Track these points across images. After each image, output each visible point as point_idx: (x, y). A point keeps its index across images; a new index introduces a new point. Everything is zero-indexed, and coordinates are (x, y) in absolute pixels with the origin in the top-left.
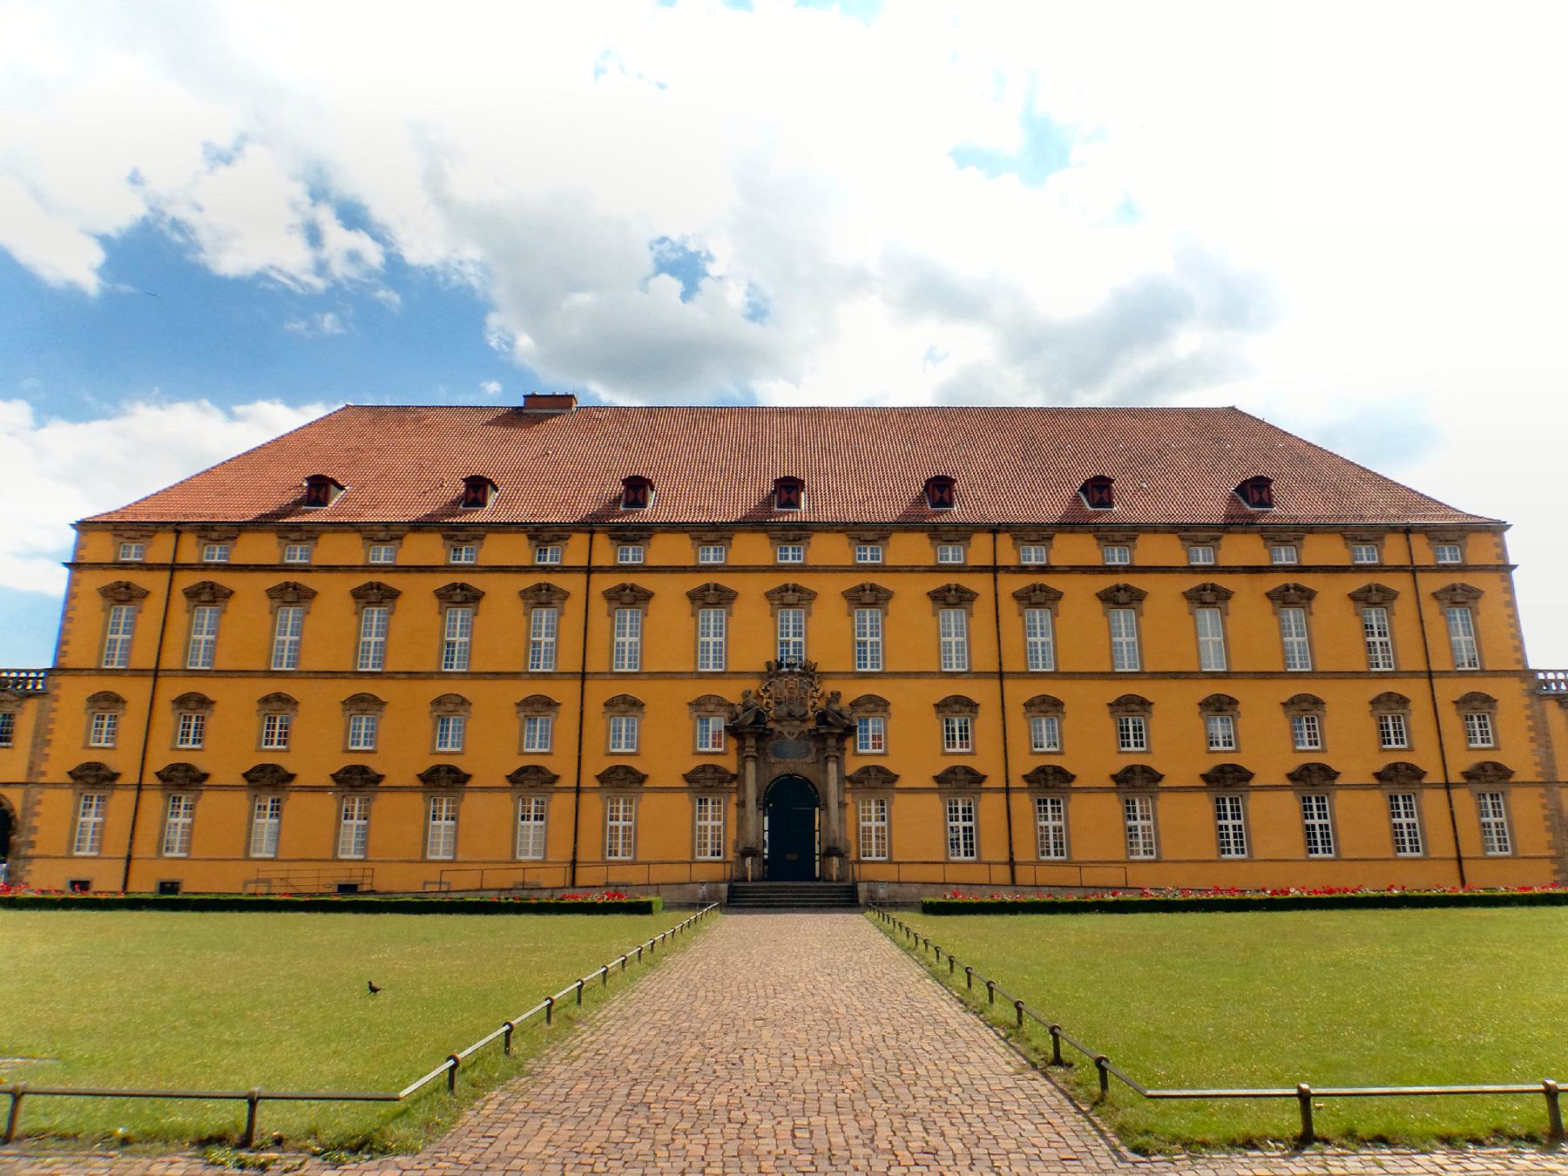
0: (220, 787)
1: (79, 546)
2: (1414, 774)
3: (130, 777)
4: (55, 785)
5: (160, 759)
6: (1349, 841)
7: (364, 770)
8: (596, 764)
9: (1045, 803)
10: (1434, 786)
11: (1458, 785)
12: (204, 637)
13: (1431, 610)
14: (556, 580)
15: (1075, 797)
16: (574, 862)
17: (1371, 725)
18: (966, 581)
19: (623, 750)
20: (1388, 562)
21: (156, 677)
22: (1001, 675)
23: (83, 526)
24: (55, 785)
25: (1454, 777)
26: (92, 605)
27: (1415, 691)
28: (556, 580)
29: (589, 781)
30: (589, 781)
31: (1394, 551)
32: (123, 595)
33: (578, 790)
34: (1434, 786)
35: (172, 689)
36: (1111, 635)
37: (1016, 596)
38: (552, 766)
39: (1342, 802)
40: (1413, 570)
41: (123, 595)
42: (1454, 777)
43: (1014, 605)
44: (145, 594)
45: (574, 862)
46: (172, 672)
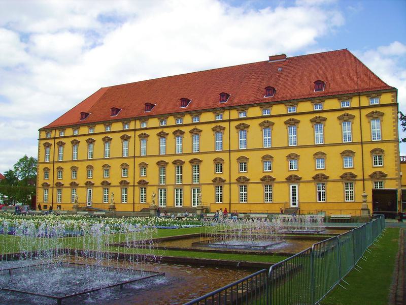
0: (65, 187)
1: (40, 136)
3: (51, 186)
4: (82, 187)
6: (329, 198)
7: (125, 181)
8: (137, 180)
9: (348, 184)
10: (360, 180)
11: (367, 180)
12: (75, 152)
15: (387, 181)
16: (134, 204)
22: (230, 151)
23: (40, 130)
24: (82, 187)
25: (366, 177)
26: (42, 147)
27: (356, 149)
29: (136, 184)
30: (136, 184)
31: (355, 102)
32: (47, 146)
34: (360, 180)
36: (182, 146)
37: (237, 127)
40: (360, 108)
41: (47, 146)
42: (366, 177)
43: (236, 130)
45: (134, 204)
46: (56, 162)
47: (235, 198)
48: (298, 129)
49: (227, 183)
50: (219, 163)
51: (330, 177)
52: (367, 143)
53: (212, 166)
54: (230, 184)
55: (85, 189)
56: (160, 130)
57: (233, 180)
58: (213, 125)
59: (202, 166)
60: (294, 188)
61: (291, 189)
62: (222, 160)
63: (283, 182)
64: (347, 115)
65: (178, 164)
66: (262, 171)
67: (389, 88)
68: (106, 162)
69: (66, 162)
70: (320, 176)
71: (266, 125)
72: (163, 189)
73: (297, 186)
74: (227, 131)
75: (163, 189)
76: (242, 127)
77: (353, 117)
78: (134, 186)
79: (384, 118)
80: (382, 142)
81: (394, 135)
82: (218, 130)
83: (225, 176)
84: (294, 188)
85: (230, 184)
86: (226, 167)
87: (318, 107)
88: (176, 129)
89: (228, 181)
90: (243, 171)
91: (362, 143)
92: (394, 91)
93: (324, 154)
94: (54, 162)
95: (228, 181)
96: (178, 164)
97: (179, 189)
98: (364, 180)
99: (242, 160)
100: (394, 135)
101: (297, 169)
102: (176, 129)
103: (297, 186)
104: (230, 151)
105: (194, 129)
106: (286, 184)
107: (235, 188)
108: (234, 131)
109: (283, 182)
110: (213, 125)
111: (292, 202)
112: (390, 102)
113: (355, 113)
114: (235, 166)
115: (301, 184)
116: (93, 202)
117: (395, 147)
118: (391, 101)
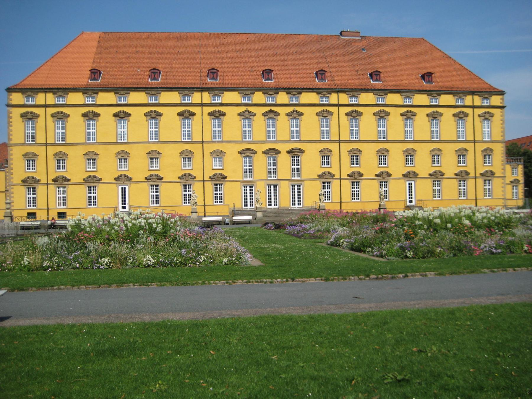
2: (467, 174)
5: (52, 176)
8: (209, 173)
10: (472, 178)
13: (477, 119)
14: (192, 109)
17: (456, 159)
18: (330, 109)
19: (218, 167)
20: (467, 104)
21: (46, 146)
28: (192, 109)
29: (207, 178)
33: (204, 181)
35: (52, 151)
38: (193, 173)
39: (445, 182)
40: (473, 107)
44: (37, 116)
47: (347, 196)
48: (415, 122)
49: (337, 179)
50: (325, 156)
51: (470, 174)
52: (479, 142)
53: (318, 159)
54: (340, 179)
55: (114, 186)
56: (242, 109)
57: (344, 175)
58: (319, 109)
59: (303, 158)
60: (410, 185)
61: (408, 185)
62: (330, 151)
63: (400, 179)
64: (463, 112)
65: (272, 153)
66: (180, 168)
67: (496, 90)
68: (154, 147)
69: (73, 144)
70: (489, 172)
71: (382, 115)
72: (249, 186)
73: (413, 183)
74: (335, 115)
75: (249, 186)
76: (354, 114)
77: (467, 115)
78: (204, 181)
79: (494, 119)
80: (492, 142)
81: (502, 136)
82: (325, 115)
83: (334, 170)
84: (410, 185)
85: (340, 179)
86: (334, 159)
87: (353, 99)
88: (267, 109)
89: (337, 176)
90: (409, 165)
91: (475, 142)
92: (501, 93)
93: (440, 150)
94: (46, 145)
95: (337, 176)
96: (272, 153)
97: (272, 186)
98: (475, 178)
99: (355, 152)
100: (502, 136)
101: (221, 168)
102: (267, 109)
103: (413, 183)
104: (340, 141)
105: (294, 111)
106: (403, 181)
107: (347, 184)
108: (344, 119)
109: (400, 179)
110: (319, 109)
111: (408, 200)
112: (499, 104)
113: (469, 111)
114: (346, 159)
115: (418, 181)
116: (132, 204)
117: (502, 147)
118: (499, 103)
